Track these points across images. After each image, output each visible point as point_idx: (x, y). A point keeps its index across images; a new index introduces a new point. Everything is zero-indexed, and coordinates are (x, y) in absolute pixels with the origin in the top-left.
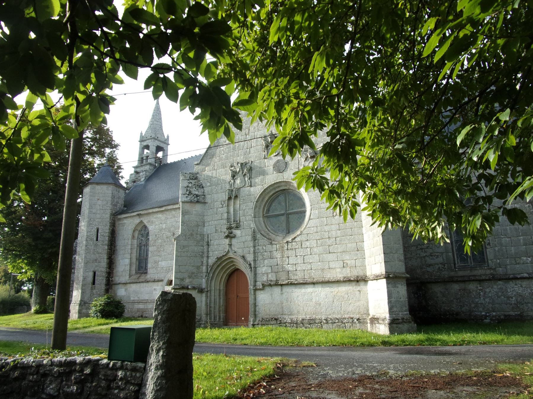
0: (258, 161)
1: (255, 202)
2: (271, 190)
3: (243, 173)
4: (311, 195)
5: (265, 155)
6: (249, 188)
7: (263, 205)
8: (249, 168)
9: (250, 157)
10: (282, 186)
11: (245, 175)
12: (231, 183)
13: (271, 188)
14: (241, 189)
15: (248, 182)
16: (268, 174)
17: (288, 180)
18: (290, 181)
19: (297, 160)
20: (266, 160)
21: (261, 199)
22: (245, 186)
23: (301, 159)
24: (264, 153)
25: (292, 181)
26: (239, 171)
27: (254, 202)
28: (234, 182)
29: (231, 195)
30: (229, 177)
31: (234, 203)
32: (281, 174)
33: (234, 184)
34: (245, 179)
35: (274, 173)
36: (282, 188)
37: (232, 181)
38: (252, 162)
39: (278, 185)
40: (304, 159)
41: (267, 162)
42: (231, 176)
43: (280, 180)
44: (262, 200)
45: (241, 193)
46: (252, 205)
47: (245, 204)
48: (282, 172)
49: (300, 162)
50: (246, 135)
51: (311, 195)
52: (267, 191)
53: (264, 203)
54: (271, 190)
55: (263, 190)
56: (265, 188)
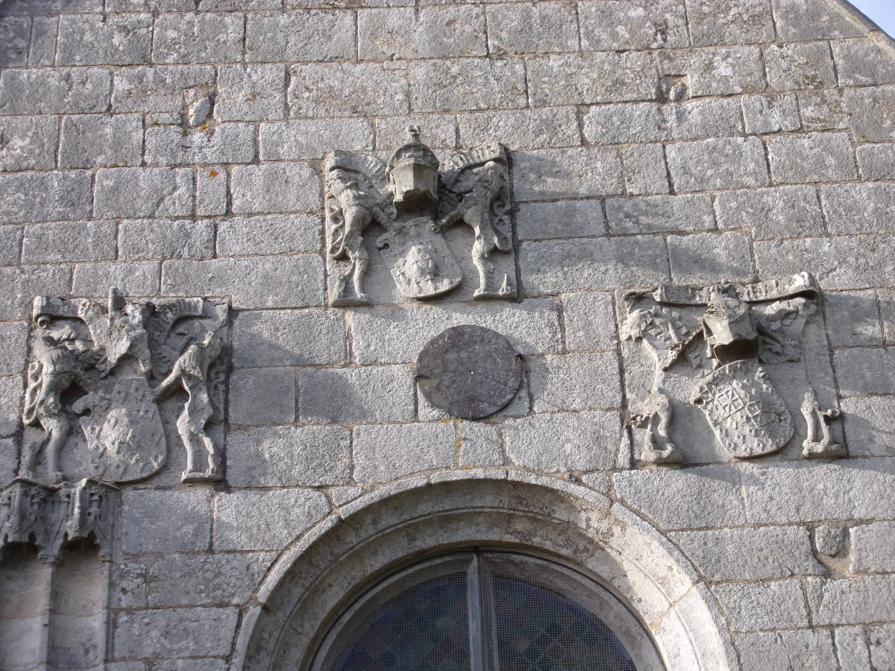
0: (285, 315)
1: (254, 611)
2: (385, 538)
3: (152, 377)
4: (736, 610)
5: (346, 281)
6: (201, 493)
7: (306, 641)
8: (215, 353)
9: (219, 279)
10: (470, 517)
11: (176, 391)
12: (32, 437)
13: (389, 520)
14: (129, 494)
15: (199, 454)
16: (364, 415)
17: (543, 481)
18: (558, 485)
19: (610, 355)
20: (351, 318)
21: (297, 592)
22: (164, 480)
23: (637, 354)
24: (336, 272)
25: (573, 489)
26: (127, 359)
27: (241, 611)
28: (71, 432)
29: (39, 529)
30: (530, 279)
31: (55, 595)
32: (480, 428)
33: (61, 447)
34: (168, 424)
35: (426, 411)
36: (464, 534)
37: (53, 427)
38: (232, 312)
39: (448, 504)
40: (672, 355)
41: (362, 329)
42: (53, 388)
43: (480, 474)
44: (305, 605)
45: (125, 525)
46: (227, 633)
47: (161, 618)
48: (486, 418)
49: (633, 371)
50: (183, 123)
51: (736, 610)
52: (352, 539)
53: (310, 628)
54: (385, 538)
55: (327, 524)
56: (343, 512)
